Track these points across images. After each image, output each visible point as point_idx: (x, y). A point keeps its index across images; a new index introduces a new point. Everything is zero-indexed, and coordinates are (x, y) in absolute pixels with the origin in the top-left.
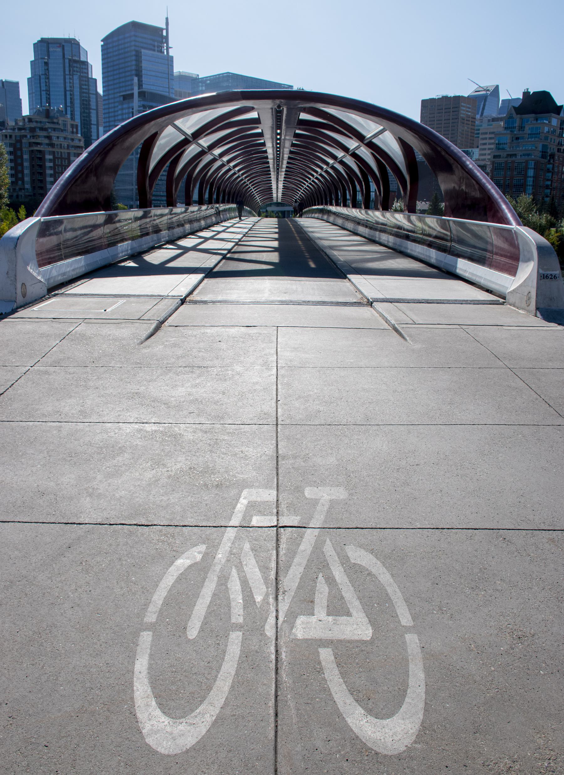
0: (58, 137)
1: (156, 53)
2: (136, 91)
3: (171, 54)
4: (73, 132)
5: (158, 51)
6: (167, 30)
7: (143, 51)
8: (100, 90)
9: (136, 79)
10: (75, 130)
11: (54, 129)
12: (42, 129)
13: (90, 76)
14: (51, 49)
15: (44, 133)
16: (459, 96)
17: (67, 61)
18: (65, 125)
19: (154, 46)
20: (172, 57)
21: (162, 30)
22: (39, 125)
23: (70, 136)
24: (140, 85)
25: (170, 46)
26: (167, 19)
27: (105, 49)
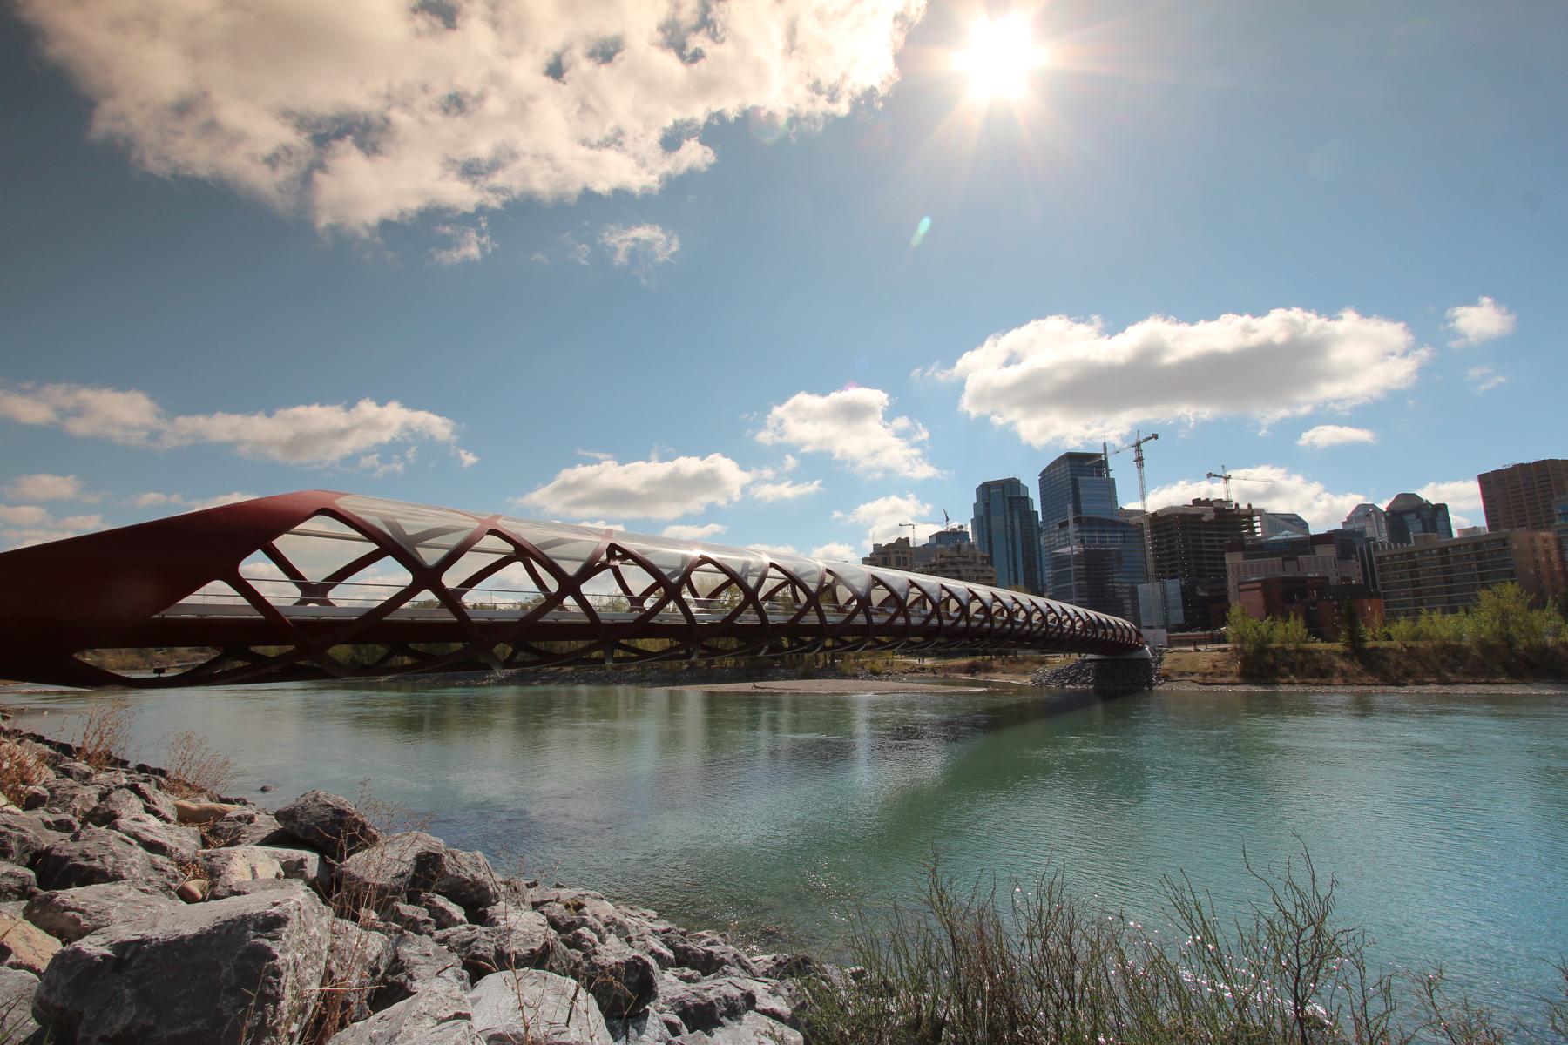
0: (967, 570)
1: (1095, 478)
2: (1071, 517)
3: (1111, 477)
4: (983, 564)
5: (1097, 476)
6: (1105, 454)
7: (1080, 478)
8: (1040, 519)
9: (1070, 506)
10: (985, 562)
11: (964, 563)
12: (952, 564)
13: (1031, 510)
14: (992, 491)
15: (953, 568)
16: (1542, 466)
17: (1007, 500)
18: (974, 558)
19: (1093, 472)
20: (1113, 480)
21: (1100, 455)
22: (949, 560)
23: (980, 568)
24: (1077, 509)
25: (1110, 469)
26: (1105, 444)
27: (1042, 482)
